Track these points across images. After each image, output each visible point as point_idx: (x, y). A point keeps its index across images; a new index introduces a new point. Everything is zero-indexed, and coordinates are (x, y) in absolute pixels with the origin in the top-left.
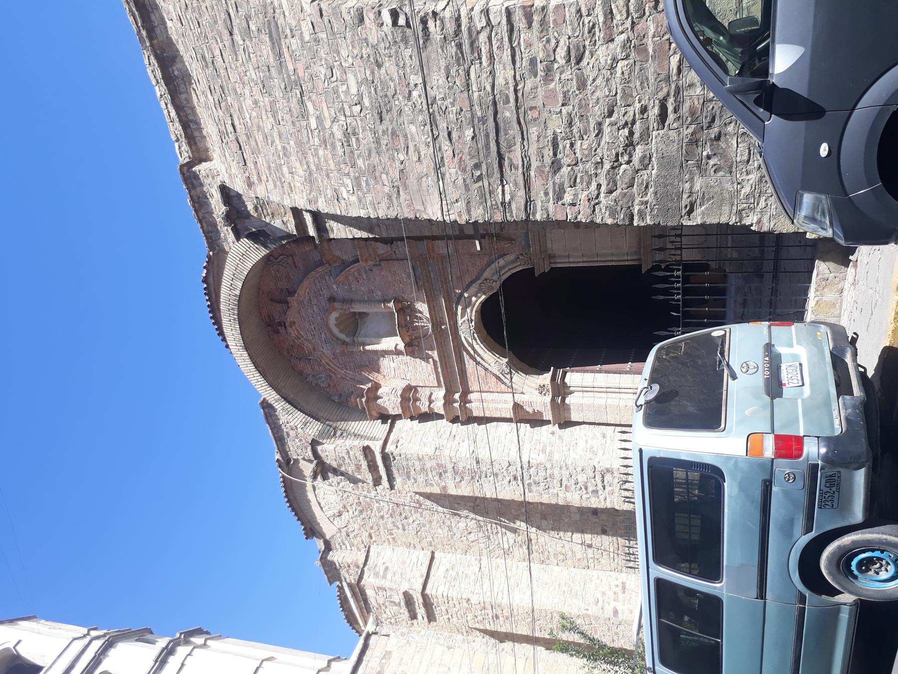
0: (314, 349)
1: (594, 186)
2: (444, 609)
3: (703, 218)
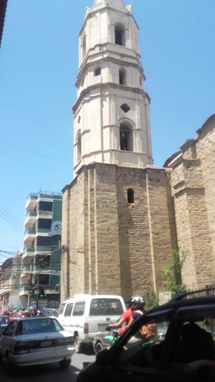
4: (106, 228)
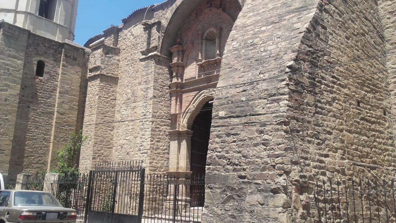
0: (200, 21)
1: (220, 150)
2: (94, 84)
3: (207, 192)
4: (4, 97)
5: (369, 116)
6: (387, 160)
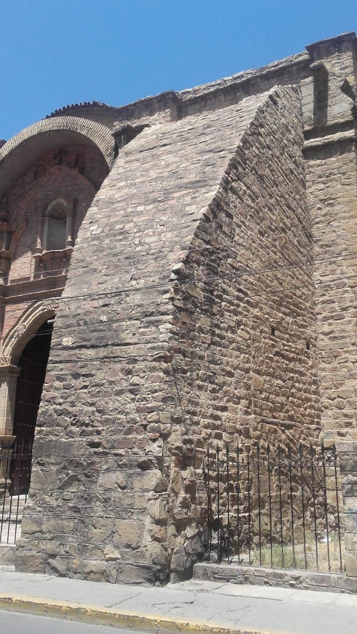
1: (62, 401)
3: (34, 471)
5: (287, 350)
6: (309, 415)
